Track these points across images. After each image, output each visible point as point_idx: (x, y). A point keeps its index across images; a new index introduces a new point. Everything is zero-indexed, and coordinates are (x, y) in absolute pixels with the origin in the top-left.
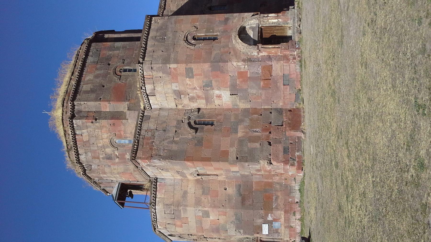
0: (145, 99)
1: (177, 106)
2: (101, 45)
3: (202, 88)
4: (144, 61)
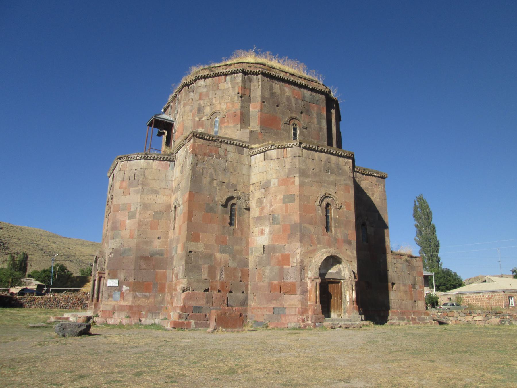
0: (261, 149)
1: (253, 184)
2: (323, 105)
3: (271, 213)
4: (302, 148)
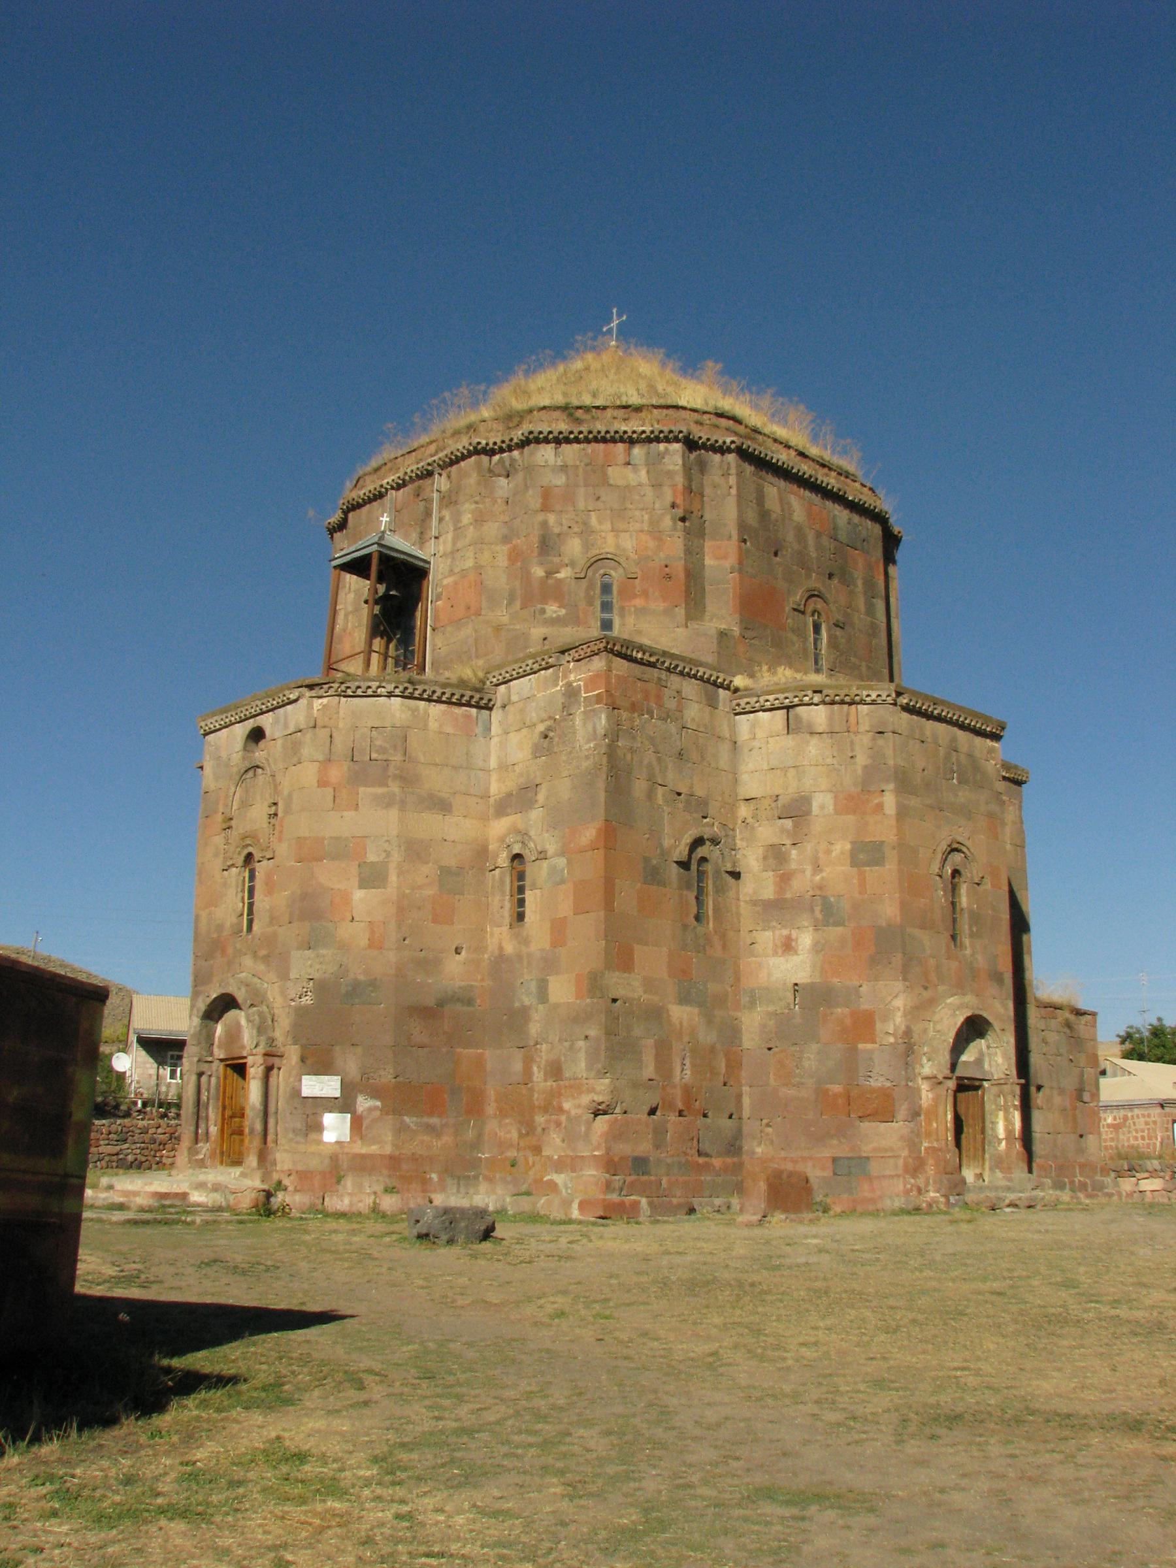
2: (878, 553)
3: (818, 893)
4: (899, 708)
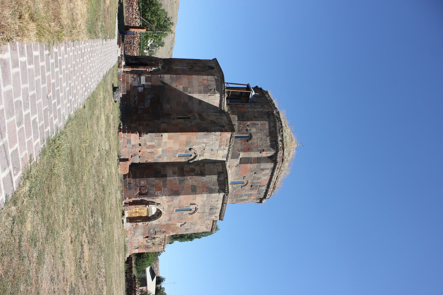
1: (204, 165)
